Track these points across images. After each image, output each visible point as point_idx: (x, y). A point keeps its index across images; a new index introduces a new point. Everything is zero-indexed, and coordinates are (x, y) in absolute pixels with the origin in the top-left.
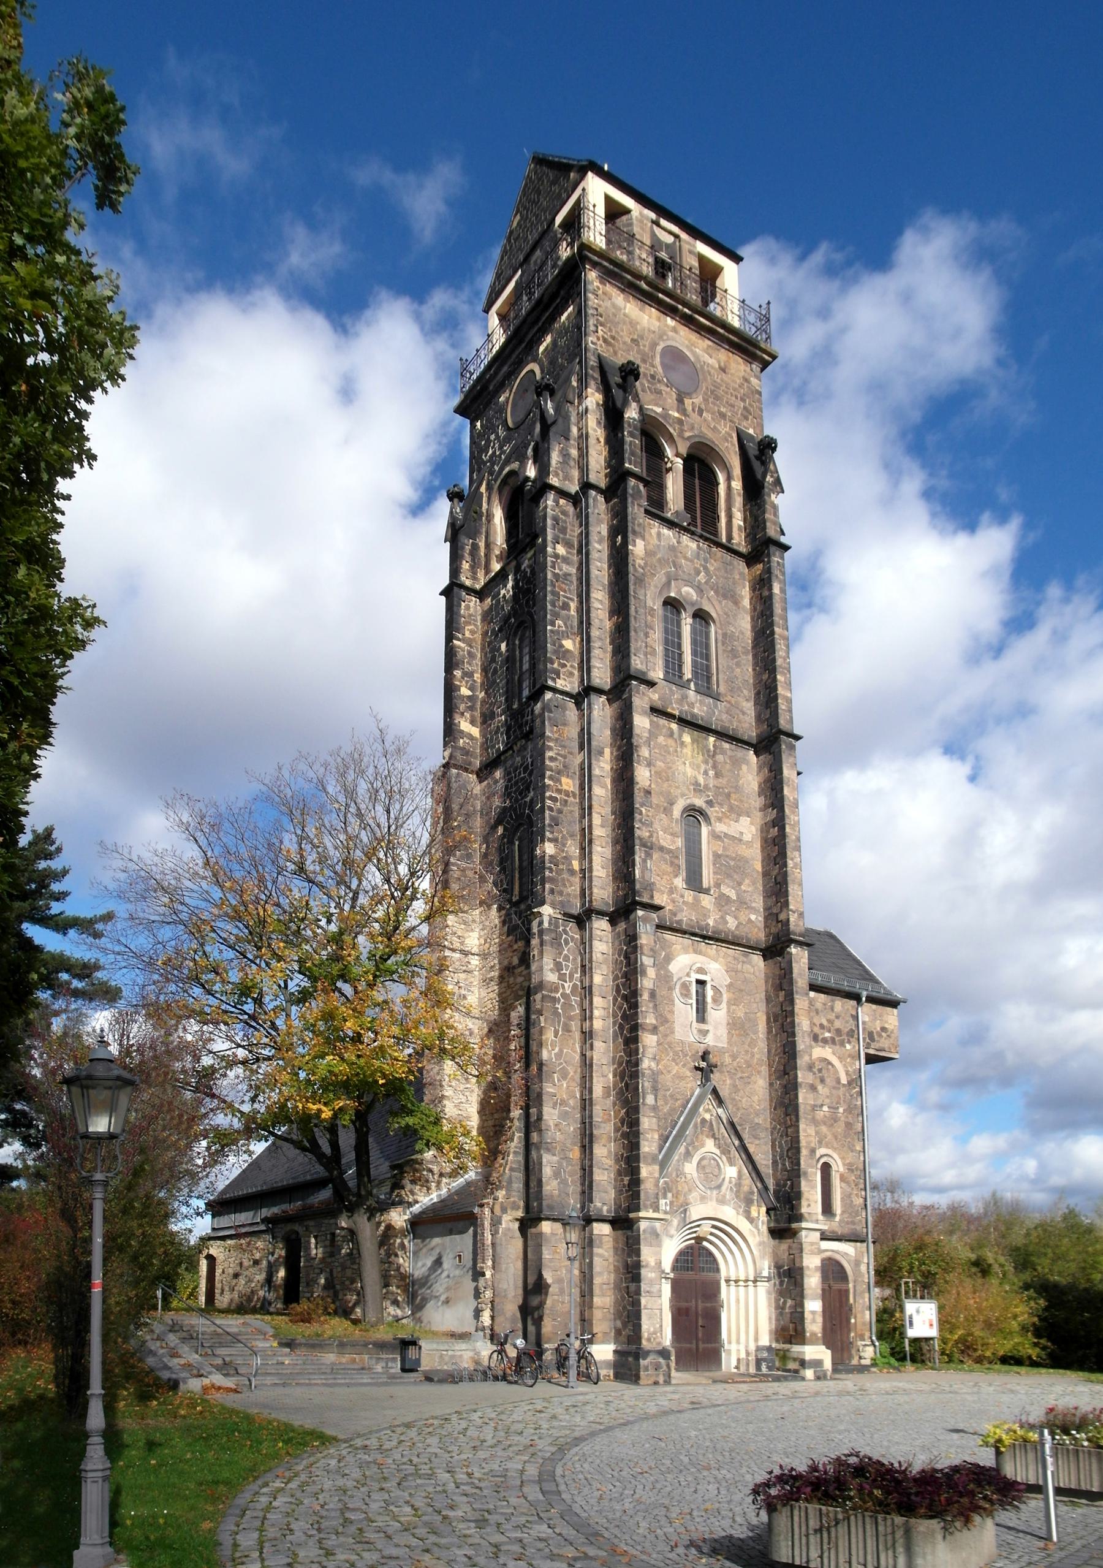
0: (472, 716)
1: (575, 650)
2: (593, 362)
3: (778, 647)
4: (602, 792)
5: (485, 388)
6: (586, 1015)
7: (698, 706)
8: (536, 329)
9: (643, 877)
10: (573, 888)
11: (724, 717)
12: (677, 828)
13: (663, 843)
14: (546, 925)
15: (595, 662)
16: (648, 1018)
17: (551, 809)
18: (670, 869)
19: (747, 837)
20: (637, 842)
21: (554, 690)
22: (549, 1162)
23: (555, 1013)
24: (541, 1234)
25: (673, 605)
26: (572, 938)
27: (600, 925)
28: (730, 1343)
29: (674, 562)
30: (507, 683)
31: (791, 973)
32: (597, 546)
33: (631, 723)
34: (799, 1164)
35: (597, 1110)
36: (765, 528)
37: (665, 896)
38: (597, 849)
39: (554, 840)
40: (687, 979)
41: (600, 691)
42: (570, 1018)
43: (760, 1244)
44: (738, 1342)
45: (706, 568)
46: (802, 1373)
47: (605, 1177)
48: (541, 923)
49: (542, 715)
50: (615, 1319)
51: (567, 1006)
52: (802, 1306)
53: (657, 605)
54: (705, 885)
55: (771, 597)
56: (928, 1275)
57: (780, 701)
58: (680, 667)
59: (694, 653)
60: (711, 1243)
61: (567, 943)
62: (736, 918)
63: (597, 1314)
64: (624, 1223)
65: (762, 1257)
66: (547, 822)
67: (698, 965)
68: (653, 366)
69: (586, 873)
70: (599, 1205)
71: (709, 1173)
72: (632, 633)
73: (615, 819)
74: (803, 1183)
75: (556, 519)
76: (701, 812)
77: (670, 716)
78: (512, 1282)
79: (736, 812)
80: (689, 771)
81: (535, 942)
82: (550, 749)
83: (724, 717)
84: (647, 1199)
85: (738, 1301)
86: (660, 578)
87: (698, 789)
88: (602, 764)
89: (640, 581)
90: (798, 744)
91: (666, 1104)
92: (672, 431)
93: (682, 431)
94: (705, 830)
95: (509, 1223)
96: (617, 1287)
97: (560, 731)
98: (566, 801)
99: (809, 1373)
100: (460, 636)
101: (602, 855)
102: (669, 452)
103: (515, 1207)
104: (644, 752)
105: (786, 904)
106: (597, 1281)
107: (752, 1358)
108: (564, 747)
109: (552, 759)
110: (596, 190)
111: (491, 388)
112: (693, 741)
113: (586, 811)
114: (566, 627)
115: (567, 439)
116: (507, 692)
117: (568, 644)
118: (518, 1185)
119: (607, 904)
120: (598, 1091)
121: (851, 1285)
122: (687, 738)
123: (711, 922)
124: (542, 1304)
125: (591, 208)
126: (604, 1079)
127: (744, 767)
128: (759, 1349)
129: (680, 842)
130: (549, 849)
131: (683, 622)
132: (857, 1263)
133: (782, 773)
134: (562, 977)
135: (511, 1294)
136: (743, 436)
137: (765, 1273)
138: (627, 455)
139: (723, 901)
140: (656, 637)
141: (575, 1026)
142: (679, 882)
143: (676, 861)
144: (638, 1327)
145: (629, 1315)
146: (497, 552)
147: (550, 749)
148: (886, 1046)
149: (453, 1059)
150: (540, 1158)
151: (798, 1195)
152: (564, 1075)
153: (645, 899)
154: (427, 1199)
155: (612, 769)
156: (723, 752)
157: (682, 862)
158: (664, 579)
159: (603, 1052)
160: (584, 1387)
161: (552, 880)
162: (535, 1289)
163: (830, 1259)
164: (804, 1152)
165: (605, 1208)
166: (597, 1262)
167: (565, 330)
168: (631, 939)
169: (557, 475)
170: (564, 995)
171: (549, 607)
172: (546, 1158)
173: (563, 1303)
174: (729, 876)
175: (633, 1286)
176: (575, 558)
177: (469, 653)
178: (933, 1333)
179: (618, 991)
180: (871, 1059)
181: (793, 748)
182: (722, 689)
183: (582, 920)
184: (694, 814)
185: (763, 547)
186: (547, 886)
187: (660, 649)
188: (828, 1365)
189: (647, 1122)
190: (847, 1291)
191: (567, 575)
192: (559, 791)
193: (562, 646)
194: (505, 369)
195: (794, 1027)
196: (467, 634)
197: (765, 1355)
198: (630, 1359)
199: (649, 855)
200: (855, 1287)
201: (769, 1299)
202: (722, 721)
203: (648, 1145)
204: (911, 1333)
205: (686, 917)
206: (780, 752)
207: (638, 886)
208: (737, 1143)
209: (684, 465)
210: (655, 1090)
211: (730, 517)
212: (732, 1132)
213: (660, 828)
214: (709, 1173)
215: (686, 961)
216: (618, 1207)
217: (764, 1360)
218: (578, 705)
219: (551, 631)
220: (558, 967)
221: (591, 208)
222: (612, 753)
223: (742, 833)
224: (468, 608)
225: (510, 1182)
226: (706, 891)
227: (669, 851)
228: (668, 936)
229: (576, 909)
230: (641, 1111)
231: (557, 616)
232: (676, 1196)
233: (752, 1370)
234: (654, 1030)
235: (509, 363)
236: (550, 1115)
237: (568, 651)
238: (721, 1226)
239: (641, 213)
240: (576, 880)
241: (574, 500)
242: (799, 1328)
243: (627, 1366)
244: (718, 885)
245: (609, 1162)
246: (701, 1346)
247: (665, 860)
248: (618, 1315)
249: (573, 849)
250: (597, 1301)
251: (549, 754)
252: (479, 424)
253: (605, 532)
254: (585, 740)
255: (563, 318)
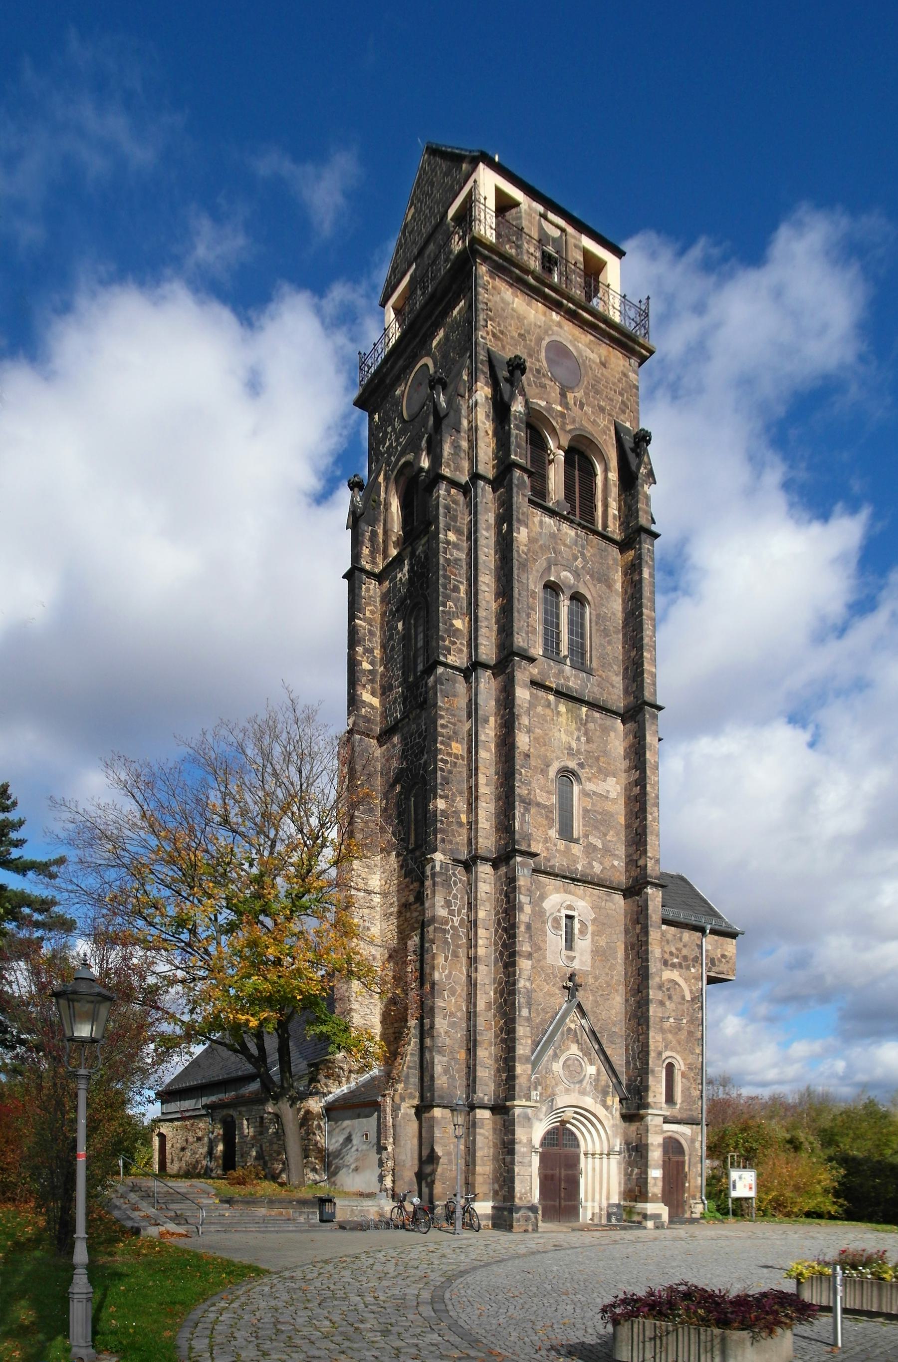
0: (372, 688)
1: (465, 629)
2: (483, 356)
3: (645, 626)
4: (487, 755)
5: (382, 381)
6: (472, 944)
7: (573, 680)
8: (429, 323)
9: (522, 829)
10: (461, 838)
11: (596, 689)
12: (552, 787)
13: (539, 799)
14: (438, 869)
15: (482, 640)
16: (524, 946)
17: (442, 770)
18: (545, 822)
19: (613, 795)
20: (517, 798)
21: (446, 665)
22: (440, 1062)
23: (445, 941)
24: (433, 1118)
25: (553, 588)
26: (460, 880)
27: (485, 870)
28: (586, 1201)
29: (554, 548)
30: (404, 658)
31: (647, 910)
32: (484, 533)
33: (514, 695)
34: (648, 1064)
35: (480, 1021)
36: (637, 517)
37: (541, 845)
38: (482, 804)
39: (445, 797)
40: (558, 914)
41: (486, 666)
42: (458, 946)
43: (613, 1126)
44: (593, 1200)
45: (583, 554)
46: (644, 1223)
47: (486, 1074)
48: (433, 867)
49: (434, 687)
50: (493, 1183)
51: (456, 936)
52: (646, 1173)
53: (539, 589)
54: (575, 836)
55: (641, 580)
56: (750, 1150)
57: (645, 675)
58: (558, 644)
59: (571, 632)
60: (573, 1125)
61: (455, 883)
62: (601, 863)
63: (479, 1180)
64: (501, 1109)
65: (615, 1136)
66: (439, 781)
67: (568, 903)
68: (539, 361)
69: (472, 825)
70: (481, 1095)
71: (573, 1071)
72: (516, 614)
73: (498, 779)
74: (651, 1079)
75: (447, 508)
76: (573, 773)
77: (548, 689)
78: (409, 1155)
79: (604, 773)
80: (564, 738)
81: (428, 883)
82: (442, 717)
83: (596, 689)
84: (521, 1091)
85: (594, 1169)
86: (541, 563)
87: (571, 753)
88: (487, 731)
89: (524, 566)
90: (660, 714)
91: (538, 1016)
92: (555, 424)
93: (564, 424)
94: (576, 788)
95: (407, 1109)
96: (495, 1159)
97: (452, 700)
98: (456, 763)
99: (650, 1224)
100: (361, 616)
101: (487, 809)
102: (552, 444)
103: (412, 1097)
104: (525, 720)
105: (645, 852)
106: (479, 1154)
107: (604, 1213)
108: (454, 715)
109: (443, 726)
110: (487, 182)
111: (388, 381)
112: (568, 711)
113: (473, 771)
114: (457, 608)
115: (458, 431)
116: (403, 667)
117: (458, 623)
118: (414, 1080)
119: (491, 851)
120: (481, 1005)
121: (687, 1158)
122: (562, 708)
123: (580, 868)
124: (433, 1172)
125: (482, 201)
126: (486, 995)
127: (612, 734)
128: (609, 1206)
129: (554, 799)
130: (441, 804)
131: (561, 604)
132: (693, 1141)
133: (645, 740)
134: (451, 913)
135: (409, 1163)
136: (620, 429)
137: (617, 1149)
138: (513, 447)
139: (590, 849)
140: (537, 617)
141: (462, 952)
142: (553, 833)
143: (551, 815)
144: (512, 1189)
145: (505, 1180)
146: (394, 539)
147: (442, 717)
148: (725, 970)
149: (359, 979)
150: (433, 1058)
151: (646, 1089)
152: (453, 992)
153: (523, 848)
154: (339, 1090)
155: (496, 735)
156: (594, 721)
157: (556, 816)
158: (545, 565)
159: (486, 975)
160: (468, 1234)
161: (443, 831)
162: (428, 1159)
163: (670, 1137)
164: (652, 1054)
165: (486, 1098)
166: (480, 1140)
167: (456, 325)
168: (511, 880)
169: (448, 466)
170: (453, 927)
171: (441, 590)
172: (437, 1058)
173: (451, 1170)
174: (596, 828)
175: (508, 1158)
176: (465, 545)
177: (370, 631)
178: (752, 1194)
179: (499, 924)
180: (711, 981)
181: (655, 717)
182: (595, 665)
183: (468, 865)
184: (567, 775)
185: (635, 535)
186: (439, 836)
187: (540, 628)
188: (665, 1217)
189: (522, 1030)
190: (683, 1162)
191: (457, 560)
192: (449, 755)
193: (453, 625)
194: (401, 363)
195: (648, 954)
196: (368, 614)
197: (615, 1210)
198: (505, 1213)
199: (527, 810)
200: (690, 1159)
201: (619, 1168)
202: (594, 693)
203: (523, 1048)
204: (734, 1194)
205: (558, 863)
206: (644, 720)
207: (517, 837)
208: (596, 1047)
209: (565, 457)
210: (529, 1005)
211: (606, 506)
212: (592, 1039)
213: (538, 787)
214: (573, 1071)
215: (557, 899)
216: (497, 1097)
217: (614, 1214)
218: (467, 678)
219: (443, 612)
220: (448, 904)
221: (482, 201)
222: (496, 721)
223: (608, 792)
224: (368, 590)
225: (407, 1077)
226: (576, 841)
227: (545, 807)
228: (543, 879)
229: (464, 855)
230: (517, 1021)
231: (448, 597)
232: (545, 1088)
233: (604, 1221)
234: (529, 956)
235: (404, 357)
236: (441, 1024)
237: (458, 630)
238: (582, 1112)
239: (529, 206)
240: (464, 831)
241: (465, 489)
242: (643, 1190)
243: (503, 1218)
244: (586, 836)
245: (490, 1062)
246: (563, 1203)
247: (541, 814)
248: (496, 1180)
249: (461, 804)
250: (478, 1169)
251: (441, 722)
252: (376, 416)
253: (492, 521)
254: (472, 710)
255: (455, 312)
